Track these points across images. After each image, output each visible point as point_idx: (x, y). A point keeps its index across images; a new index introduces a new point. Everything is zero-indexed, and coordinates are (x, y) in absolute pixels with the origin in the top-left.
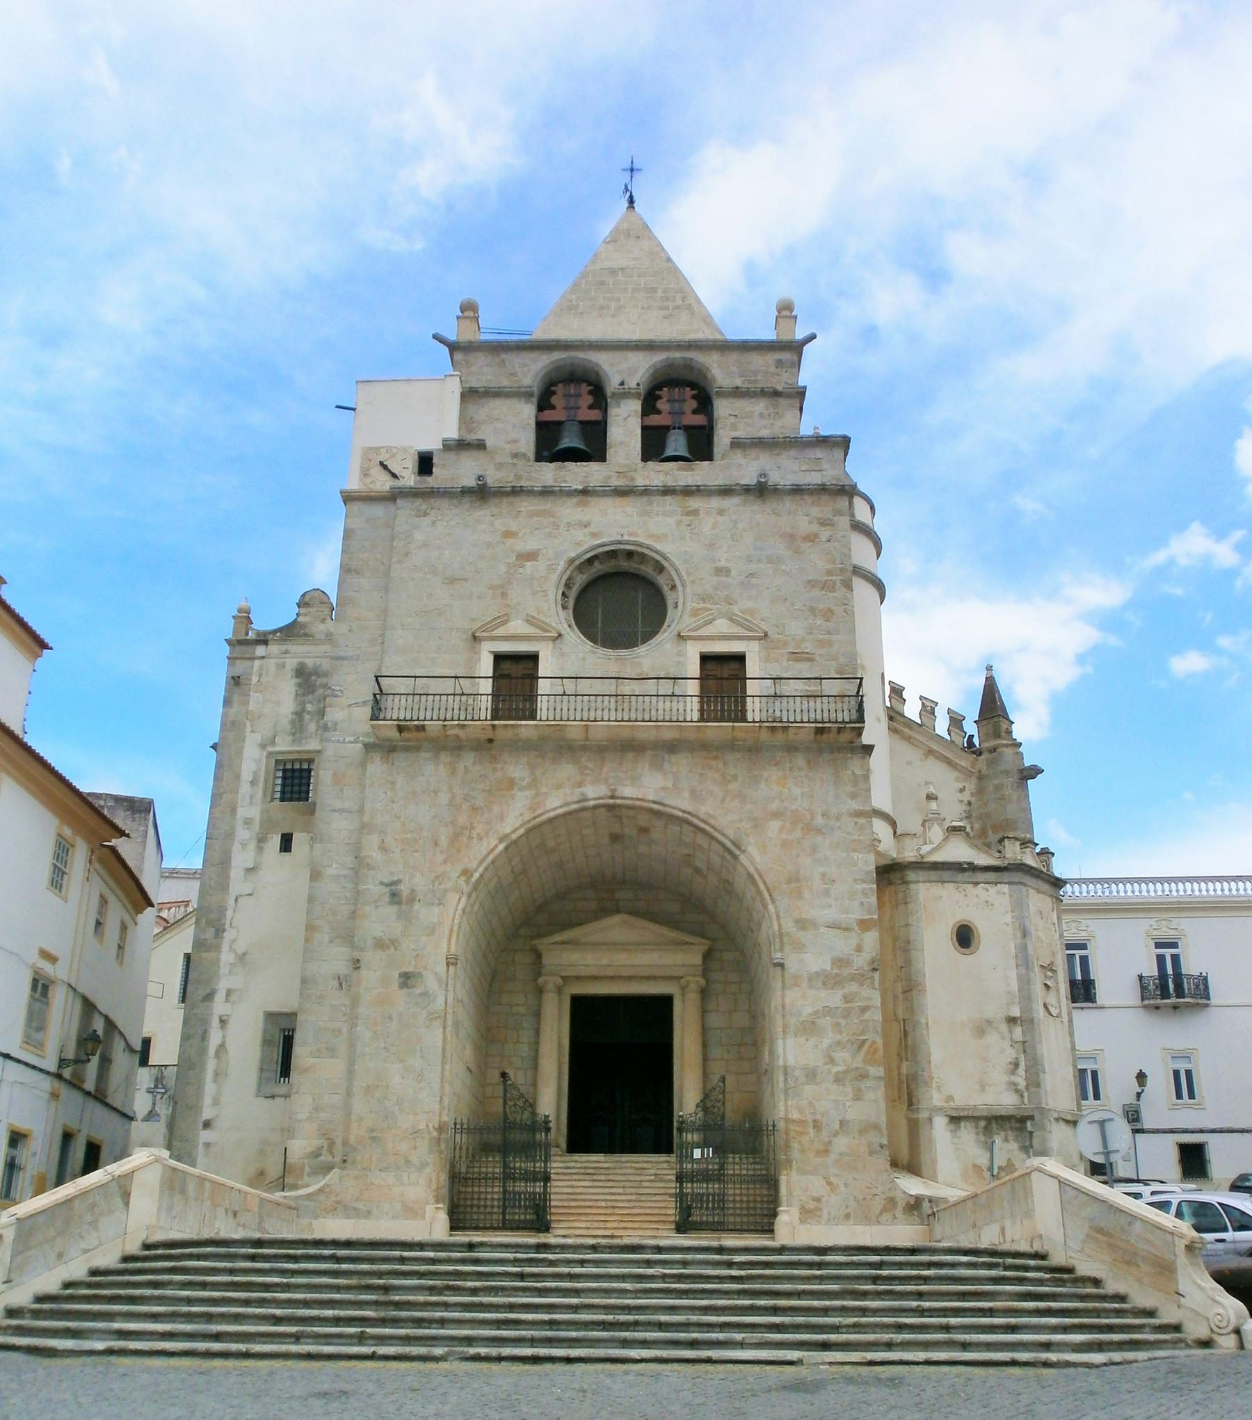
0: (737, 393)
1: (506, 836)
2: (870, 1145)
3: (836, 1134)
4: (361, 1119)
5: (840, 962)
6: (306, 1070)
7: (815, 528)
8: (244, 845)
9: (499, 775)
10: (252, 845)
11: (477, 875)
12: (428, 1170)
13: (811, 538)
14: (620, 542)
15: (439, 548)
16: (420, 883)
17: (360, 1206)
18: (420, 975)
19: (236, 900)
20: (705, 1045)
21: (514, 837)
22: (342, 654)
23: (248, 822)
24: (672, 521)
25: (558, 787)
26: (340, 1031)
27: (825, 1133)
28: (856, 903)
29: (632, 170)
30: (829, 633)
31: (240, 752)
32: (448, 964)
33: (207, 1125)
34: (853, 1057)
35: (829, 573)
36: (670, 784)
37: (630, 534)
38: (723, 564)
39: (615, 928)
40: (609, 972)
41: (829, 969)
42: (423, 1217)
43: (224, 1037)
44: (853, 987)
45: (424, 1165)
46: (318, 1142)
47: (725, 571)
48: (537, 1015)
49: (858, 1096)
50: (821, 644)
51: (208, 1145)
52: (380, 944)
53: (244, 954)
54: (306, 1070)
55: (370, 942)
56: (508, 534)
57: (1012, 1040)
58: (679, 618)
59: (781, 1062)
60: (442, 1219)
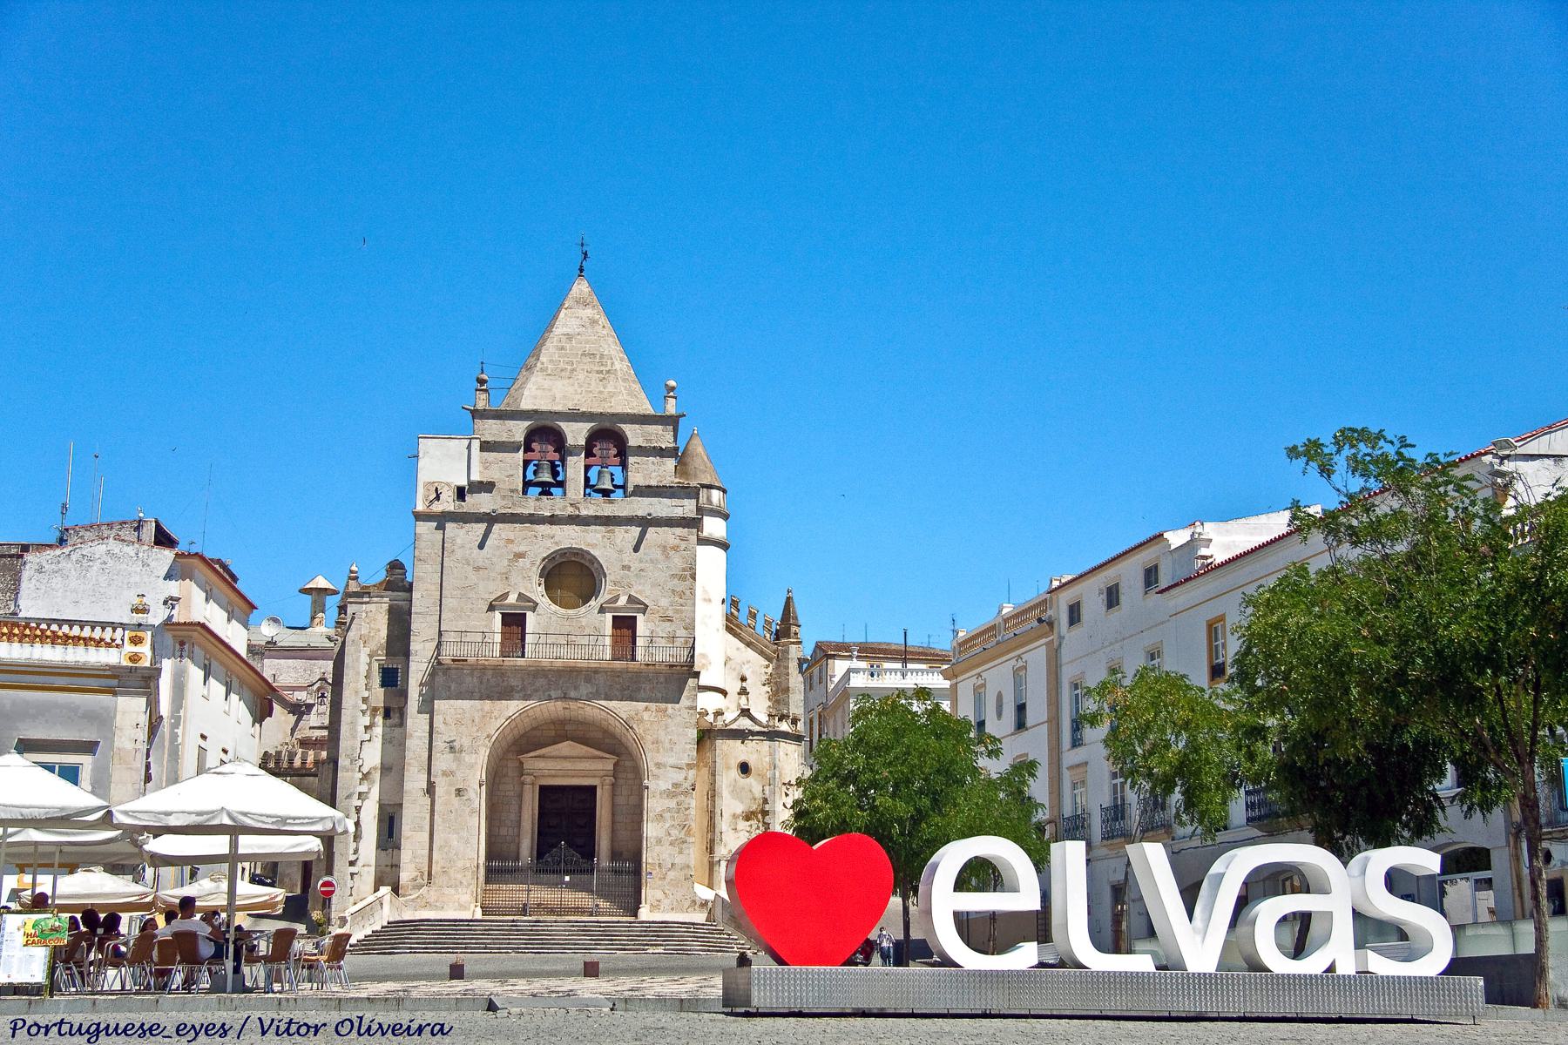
0: (642, 451)
1: (510, 717)
2: (685, 875)
3: (669, 870)
4: (437, 863)
5: (675, 785)
6: (408, 838)
7: (677, 542)
8: (364, 712)
9: (505, 683)
10: (368, 712)
11: (494, 738)
12: (471, 887)
13: (675, 548)
14: (570, 548)
15: (471, 549)
16: (466, 742)
17: (438, 904)
18: (467, 790)
19: (361, 744)
20: (613, 815)
21: (513, 717)
22: (417, 611)
23: (365, 700)
24: (599, 536)
25: (536, 691)
26: (425, 818)
27: (664, 871)
28: (686, 755)
29: (582, 245)
30: (682, 605)
31: (358, 660)
32: (480, 786)
33: (352, 863)
34: (680, 832)
35: (684, 570)
36: (594, 691)
37: (576, 544)
38: (626, 563)
39: (566, 748)
40: (561, 773)
41: (670, 787)
42: (469, 910)
43: (359, 817)
44: (683, 798)
45: (470, 885)
46: (416, 874)
47: (626, 568)
48: (520, 796)
49: (681, 852)
50: (677, 611)
51: (352, 874)
52: (445, 774)
53: (368, 773)
54: (408, 838)
55: (440, 773)
56: (510, 541)
57: (764, 822)
58: (604, 597)
59: (645, 835)
60: (479, 911)
